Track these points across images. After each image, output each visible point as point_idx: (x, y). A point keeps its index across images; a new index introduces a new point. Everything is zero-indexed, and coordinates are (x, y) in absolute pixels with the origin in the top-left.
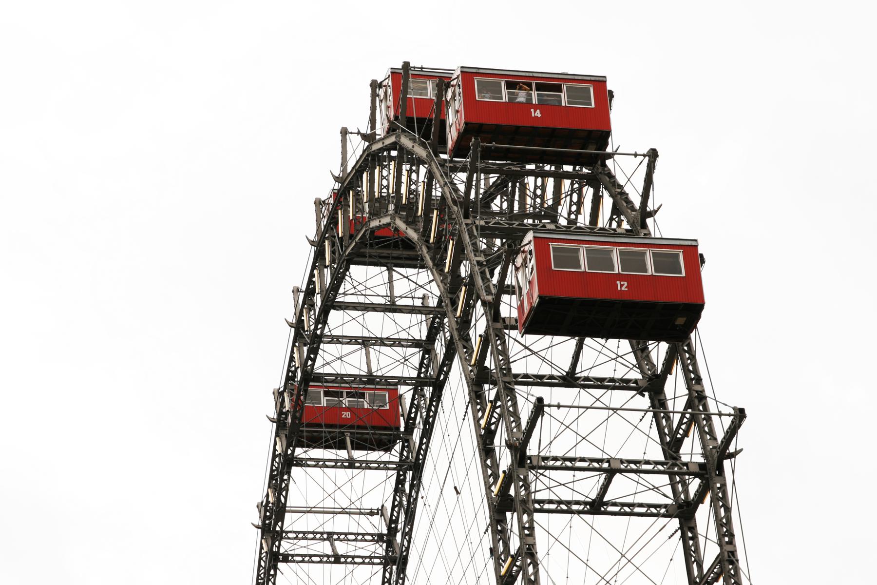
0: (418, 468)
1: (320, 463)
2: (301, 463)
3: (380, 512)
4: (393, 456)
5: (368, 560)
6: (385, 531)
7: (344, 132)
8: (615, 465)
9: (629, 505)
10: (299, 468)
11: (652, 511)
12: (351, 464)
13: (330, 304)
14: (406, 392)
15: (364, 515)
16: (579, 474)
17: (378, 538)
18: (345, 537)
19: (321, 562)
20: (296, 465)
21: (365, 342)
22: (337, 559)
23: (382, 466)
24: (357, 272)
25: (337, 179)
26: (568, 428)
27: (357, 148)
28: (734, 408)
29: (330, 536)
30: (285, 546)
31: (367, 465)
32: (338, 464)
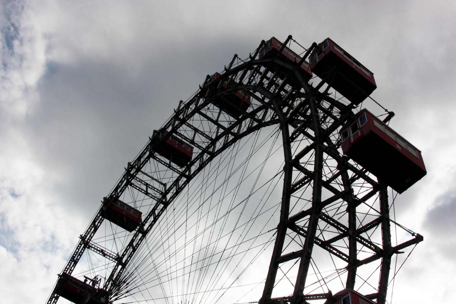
0: (189, 178)
1: (160, 161)
2: (155, 158)
3: (165, 185)
5: (153, 197)
7: (236, 56)
10: (152, 159)
12: (169, 166)
13: (197, 110)
15: (159, 183)
17: (162, 193)
18: (153, 188)
19: (139, 190)
20: (152, 158)
21: (196, 130)
22: (147, 193)
23: (178, 172)
24: (211, 106)
26: (300, 199)
29: (147, 185)
31: (174, 169)
32: (165, 164)
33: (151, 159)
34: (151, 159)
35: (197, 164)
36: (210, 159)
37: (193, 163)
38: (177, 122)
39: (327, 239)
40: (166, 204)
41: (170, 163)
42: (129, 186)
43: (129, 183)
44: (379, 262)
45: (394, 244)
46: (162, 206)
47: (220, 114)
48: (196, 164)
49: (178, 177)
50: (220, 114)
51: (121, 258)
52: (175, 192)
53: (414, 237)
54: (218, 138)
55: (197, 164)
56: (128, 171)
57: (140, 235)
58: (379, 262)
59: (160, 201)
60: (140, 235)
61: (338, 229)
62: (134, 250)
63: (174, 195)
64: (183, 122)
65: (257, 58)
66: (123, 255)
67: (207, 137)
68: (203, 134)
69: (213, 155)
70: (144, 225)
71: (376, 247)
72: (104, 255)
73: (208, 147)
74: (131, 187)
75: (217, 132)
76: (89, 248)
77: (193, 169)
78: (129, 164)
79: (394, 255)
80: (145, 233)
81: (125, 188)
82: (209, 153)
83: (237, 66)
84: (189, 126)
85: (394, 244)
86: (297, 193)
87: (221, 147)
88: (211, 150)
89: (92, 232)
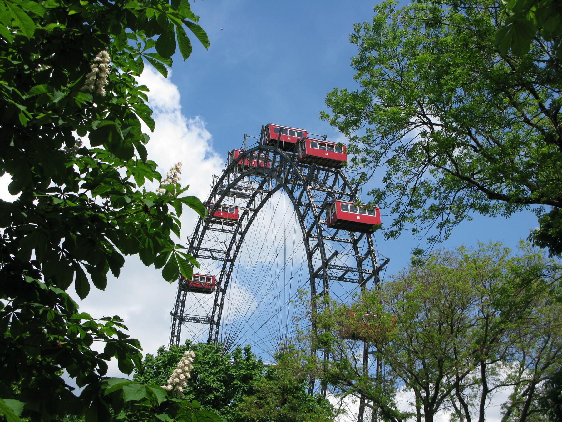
0: (243, 234)
7: (245, 136)
12: (224, 231)
28: (387, 258)
33: (207, 231)
34: (207, 231)
40: (233, 261)
53: (384, 261)
57: (221, 294)
60: (221, 294)
62: (221, 307)
63: (236, 251)
66: (213, 315)
69: (256, 211)
72: (198, 321)
76: (184, 321)
77: (244, 224)
79: (380, 272)
80: (224, 291)
87: (260, 202)
88: (252, 206)
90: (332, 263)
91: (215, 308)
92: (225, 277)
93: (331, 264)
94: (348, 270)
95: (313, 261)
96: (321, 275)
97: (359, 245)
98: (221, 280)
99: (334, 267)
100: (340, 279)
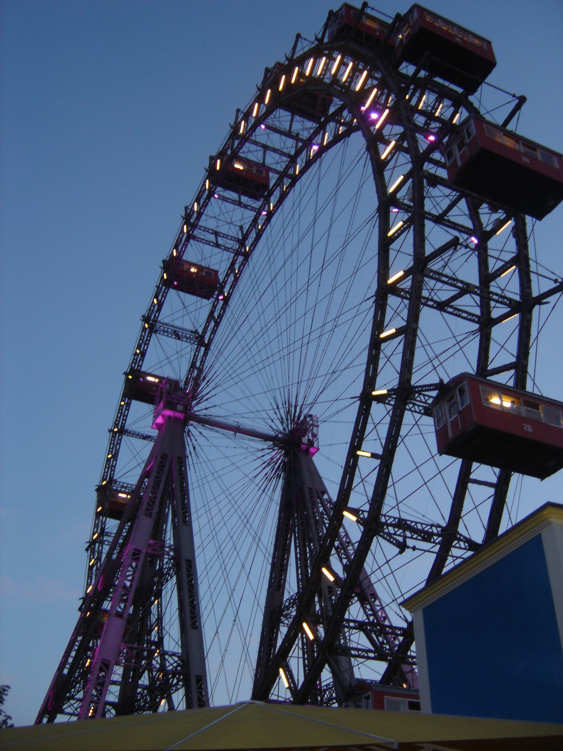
4: (257, 204)
6: (241, 237)
7: (298, 36)
8: (470, 289)
9: (459, 310)
11: (470, 317)
12: (239, 204)
14: (273, 178)
16: (439, 285)
17: (238, 241)
21: (265, 148)
22: (217, 245)
23: (253, 209)
25: (287, 59)
27: (304, 47)
29: (216, 234)
30: (196, 232)
31: (246, 206)
32: (233, 202)
35: (277, 194)
36: (292, 185)
37: (271, 193)
38: (236, 142)
39: (443, 299)
40: (247, 256)
41: (240, 198)
42: (191, 241)
43: (190, 237)
44: (516, 317)
45: (535, 294)
46: (241, 259)
47: (292, 121)
48: (275, 193)
49: (255, 216)
50: (292, 121)
51: (202, 337)
52: (254, 236)
53: (558, 284)
54: (298, 152)
55: (277, 194)
56: (187, 219)
58: (516, 317)
59: (237, 253)
61: (454, 286)
64: (245, 139)
65: (326, 40)
67: (282, 154)
68: (275, 150)
69: (295, 179)
70: (224, 287)
71: (511, 300)
72: (178, 337)
73: (287, 168)
74: (196, 242)
75: (296, 146)
76: (156, 332)
78: (186, 208)
79: (537, 307)
81: (187, 245)
82: (289, 177)
83: (301, 52)
84: (255, 143)
85: (535, 294)
86: (394, 246)
89: (157, 311)
90: (435, 265)
91: (208, 321)
92: (232, 278)
93: (435, 268)
94: (466, 289)
95: (392, 254)
96: (403, 290)
97: (492, 243)
98: (225, 282)
99: (438, 276)
100: (441, 306)
